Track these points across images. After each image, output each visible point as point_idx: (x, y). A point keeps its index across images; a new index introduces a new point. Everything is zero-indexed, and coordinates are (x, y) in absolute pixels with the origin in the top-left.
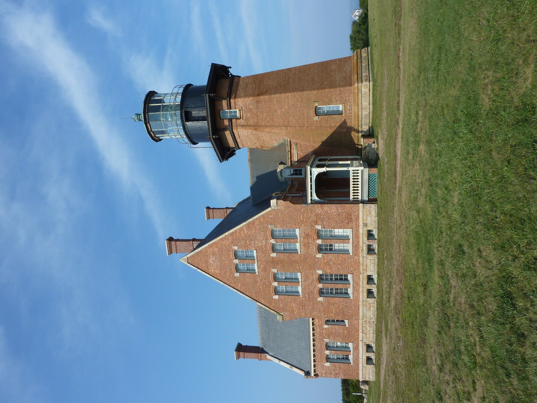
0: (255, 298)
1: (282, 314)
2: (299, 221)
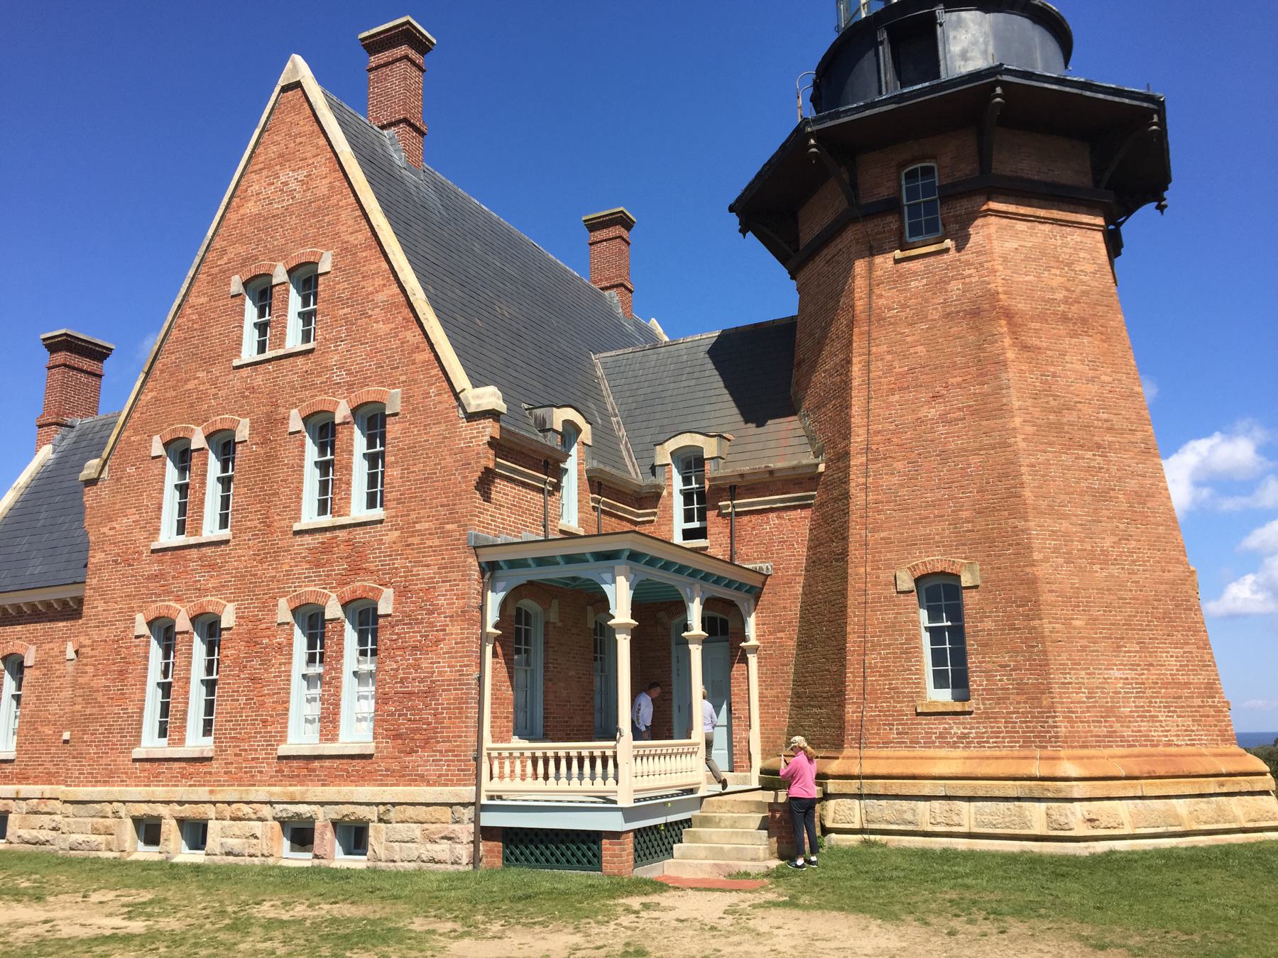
0: (158, 365)
1: (105, 475)
2: (413, 516)
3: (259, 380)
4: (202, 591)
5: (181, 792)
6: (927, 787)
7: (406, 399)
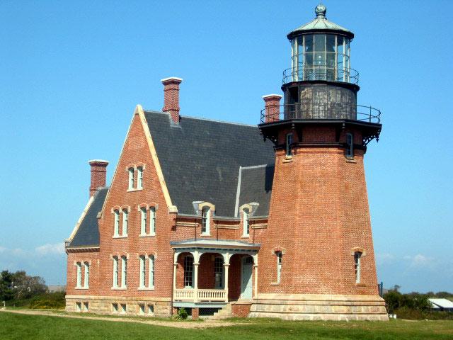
5: (120, 298)
6: (266, 302)
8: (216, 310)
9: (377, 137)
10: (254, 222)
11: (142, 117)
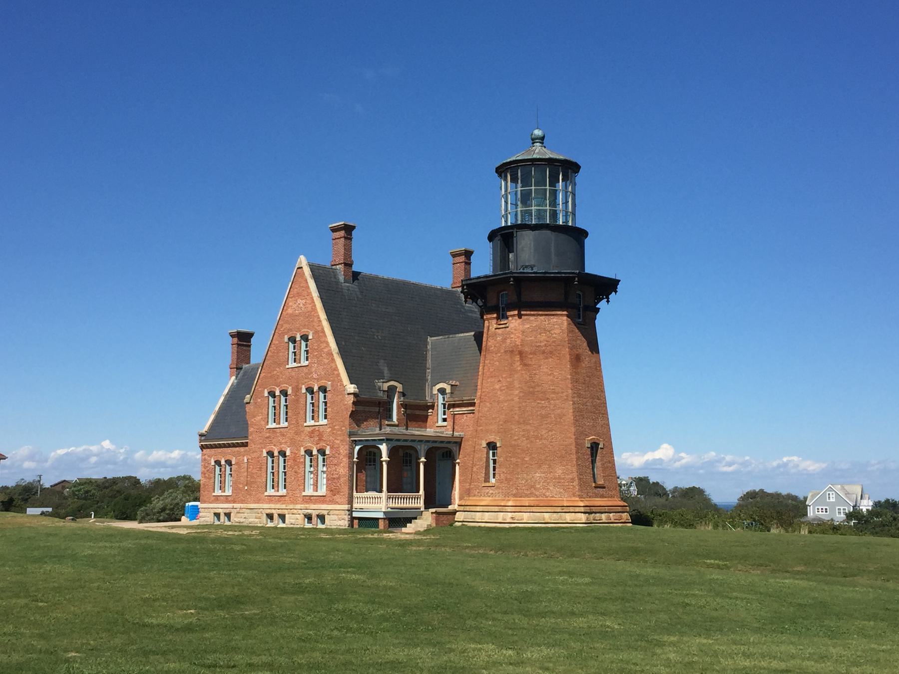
3: (293, 374)
4: (281, 443)
5: (278, 506)
6: (478, 509)
7: (332, 386)
8: (409, 520)
9: (608, 298)
10: (454, 406)
11: (307, 271)
